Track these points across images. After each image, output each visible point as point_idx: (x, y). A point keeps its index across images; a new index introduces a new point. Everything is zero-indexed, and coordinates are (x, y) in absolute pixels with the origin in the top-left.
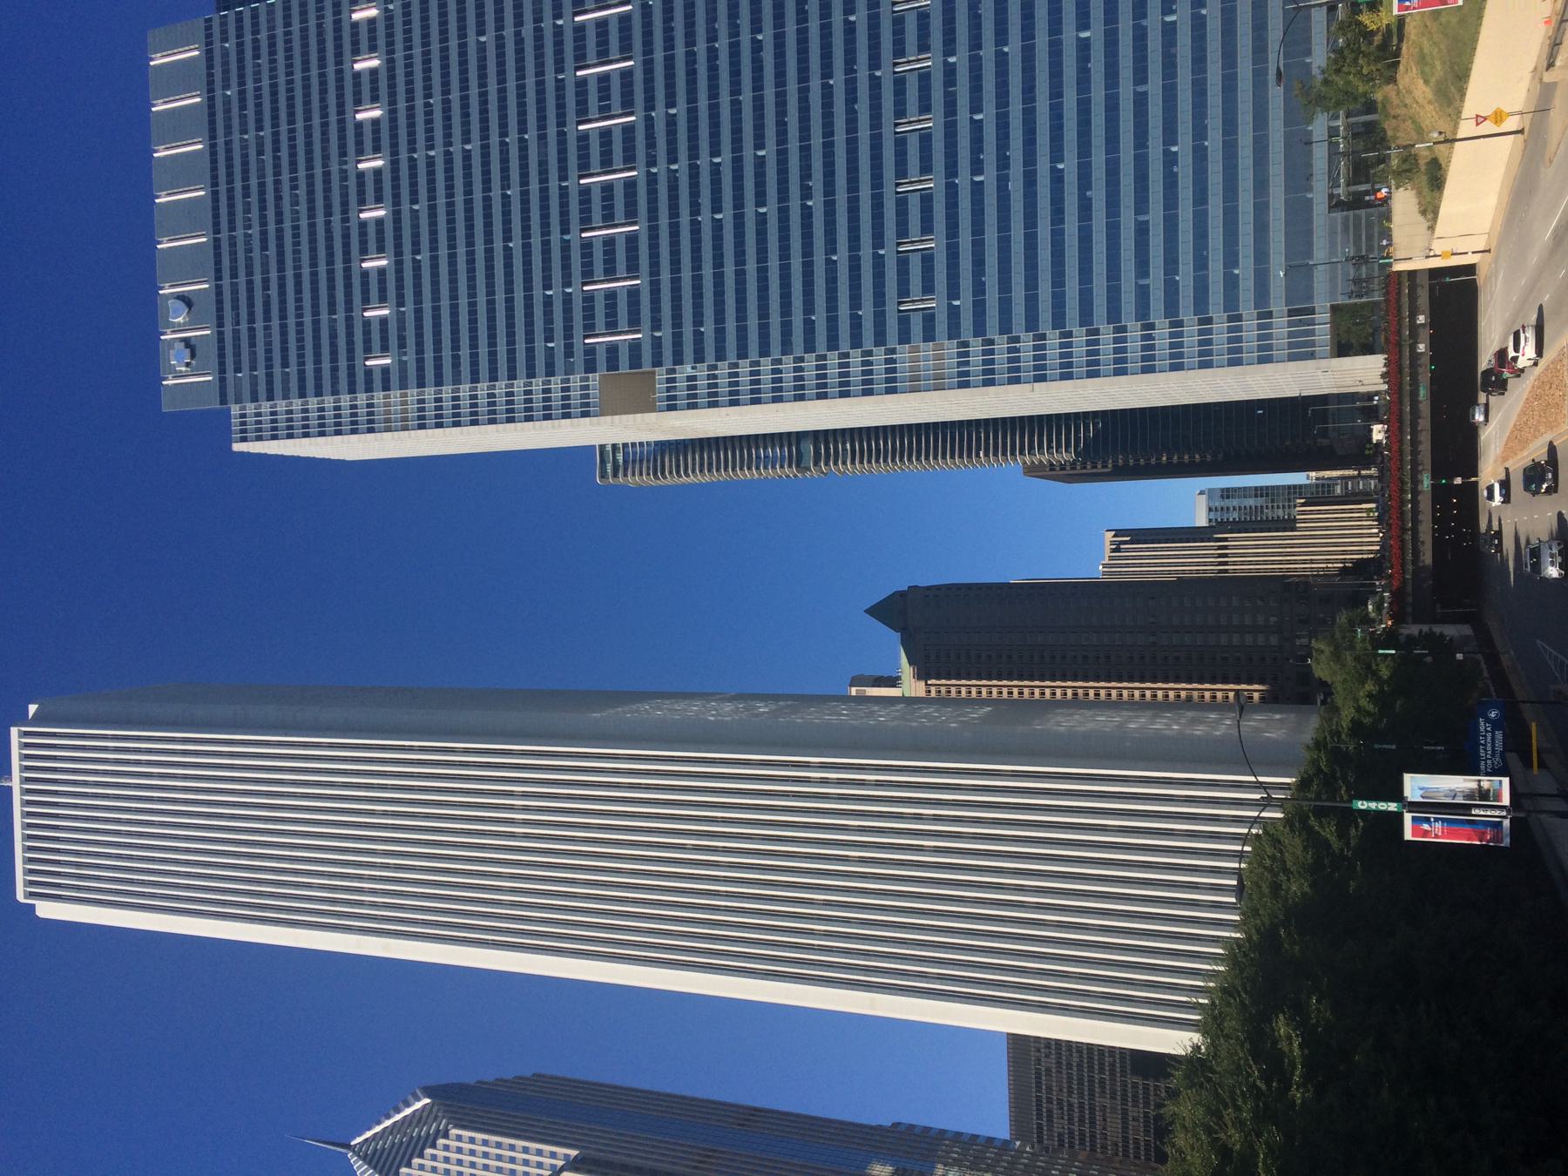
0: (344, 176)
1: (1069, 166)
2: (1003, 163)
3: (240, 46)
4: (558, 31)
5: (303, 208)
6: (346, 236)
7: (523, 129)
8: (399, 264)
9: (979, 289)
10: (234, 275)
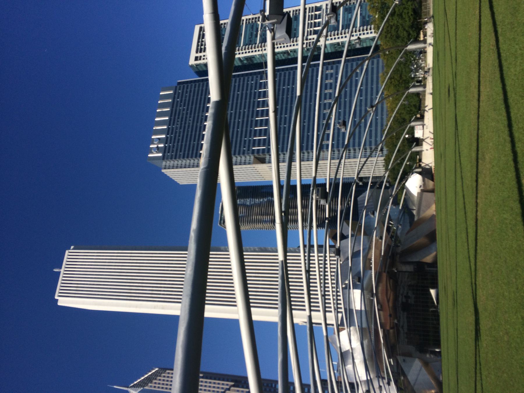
3: (183, 92)
5: (191, 122)
6: (200, 127)
7: (245, 108)
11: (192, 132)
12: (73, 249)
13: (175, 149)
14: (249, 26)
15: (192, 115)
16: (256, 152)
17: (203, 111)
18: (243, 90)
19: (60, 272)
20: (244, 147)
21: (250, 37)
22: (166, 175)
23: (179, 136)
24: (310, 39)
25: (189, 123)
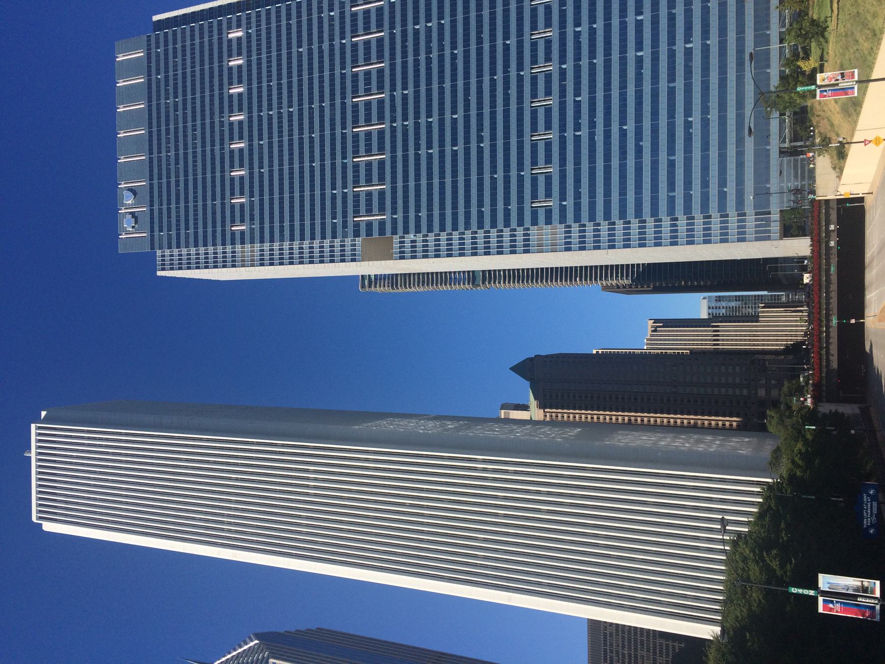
0: (222, 124)
1: (630, 127)
2: (592, 125)
3: (166, 52)
4: (343, 46)
5: (199, 142)
7: (322, 100)
8: (251, 174)
9: (578, 195)
10: (160, 178)
17: (222, 112)
18: (310, 43)
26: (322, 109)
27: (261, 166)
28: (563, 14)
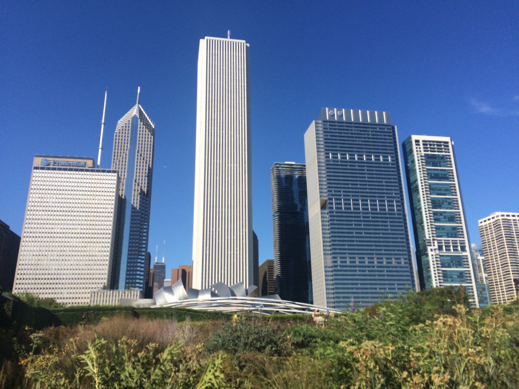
0: (363, 152)
1: (359, 286)
2: (360, 275)
3: (385, 132)
5: (357, 143)
6: (352, 151)
7: (369, 189)
9: (341, 271)
10: (346, 126)
11: (348, 144)
12: (246, 46)
13: (332, 131)
14: (448, 187)
15: (364, 143)
16: (331, 201)
17: (367, 152)
19: (226, 37)
20: (335, 191)
21: (437, 189)
22: (310, 124)
23: (344, 133)
24: (434, 243)
25: (356, 141)
26: (366, 189)
27: (350, 166)
28: (389, 267)
